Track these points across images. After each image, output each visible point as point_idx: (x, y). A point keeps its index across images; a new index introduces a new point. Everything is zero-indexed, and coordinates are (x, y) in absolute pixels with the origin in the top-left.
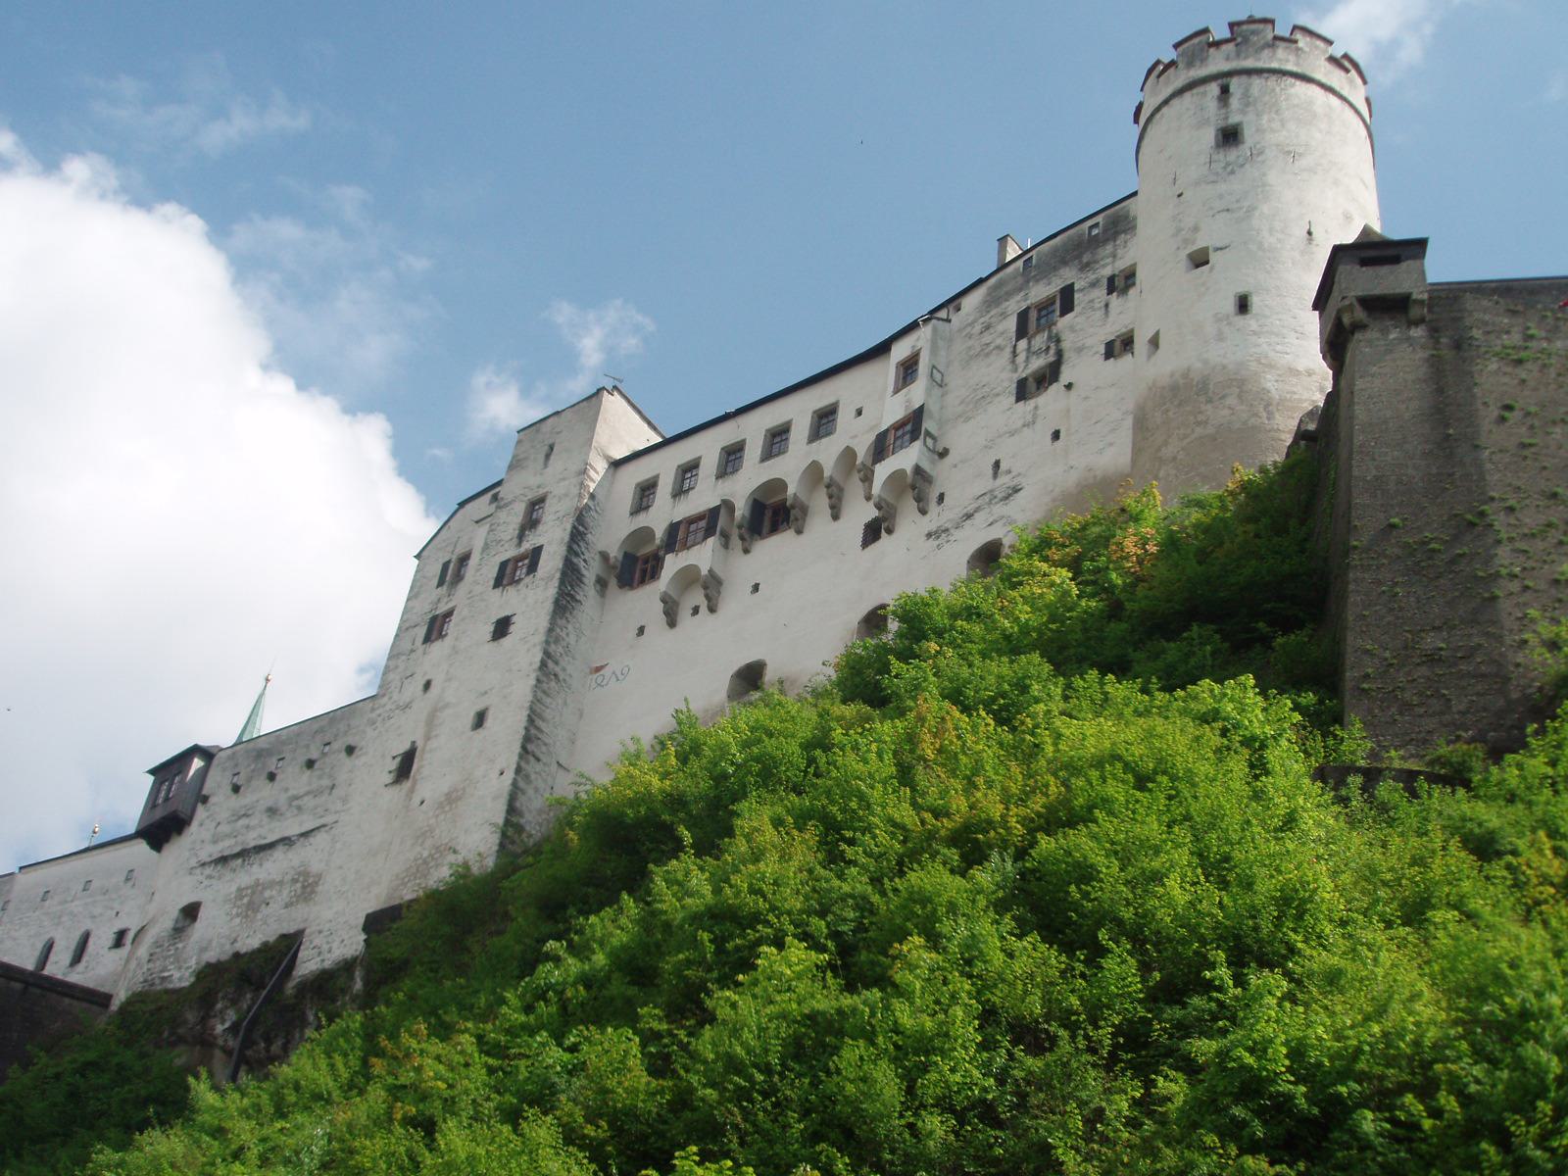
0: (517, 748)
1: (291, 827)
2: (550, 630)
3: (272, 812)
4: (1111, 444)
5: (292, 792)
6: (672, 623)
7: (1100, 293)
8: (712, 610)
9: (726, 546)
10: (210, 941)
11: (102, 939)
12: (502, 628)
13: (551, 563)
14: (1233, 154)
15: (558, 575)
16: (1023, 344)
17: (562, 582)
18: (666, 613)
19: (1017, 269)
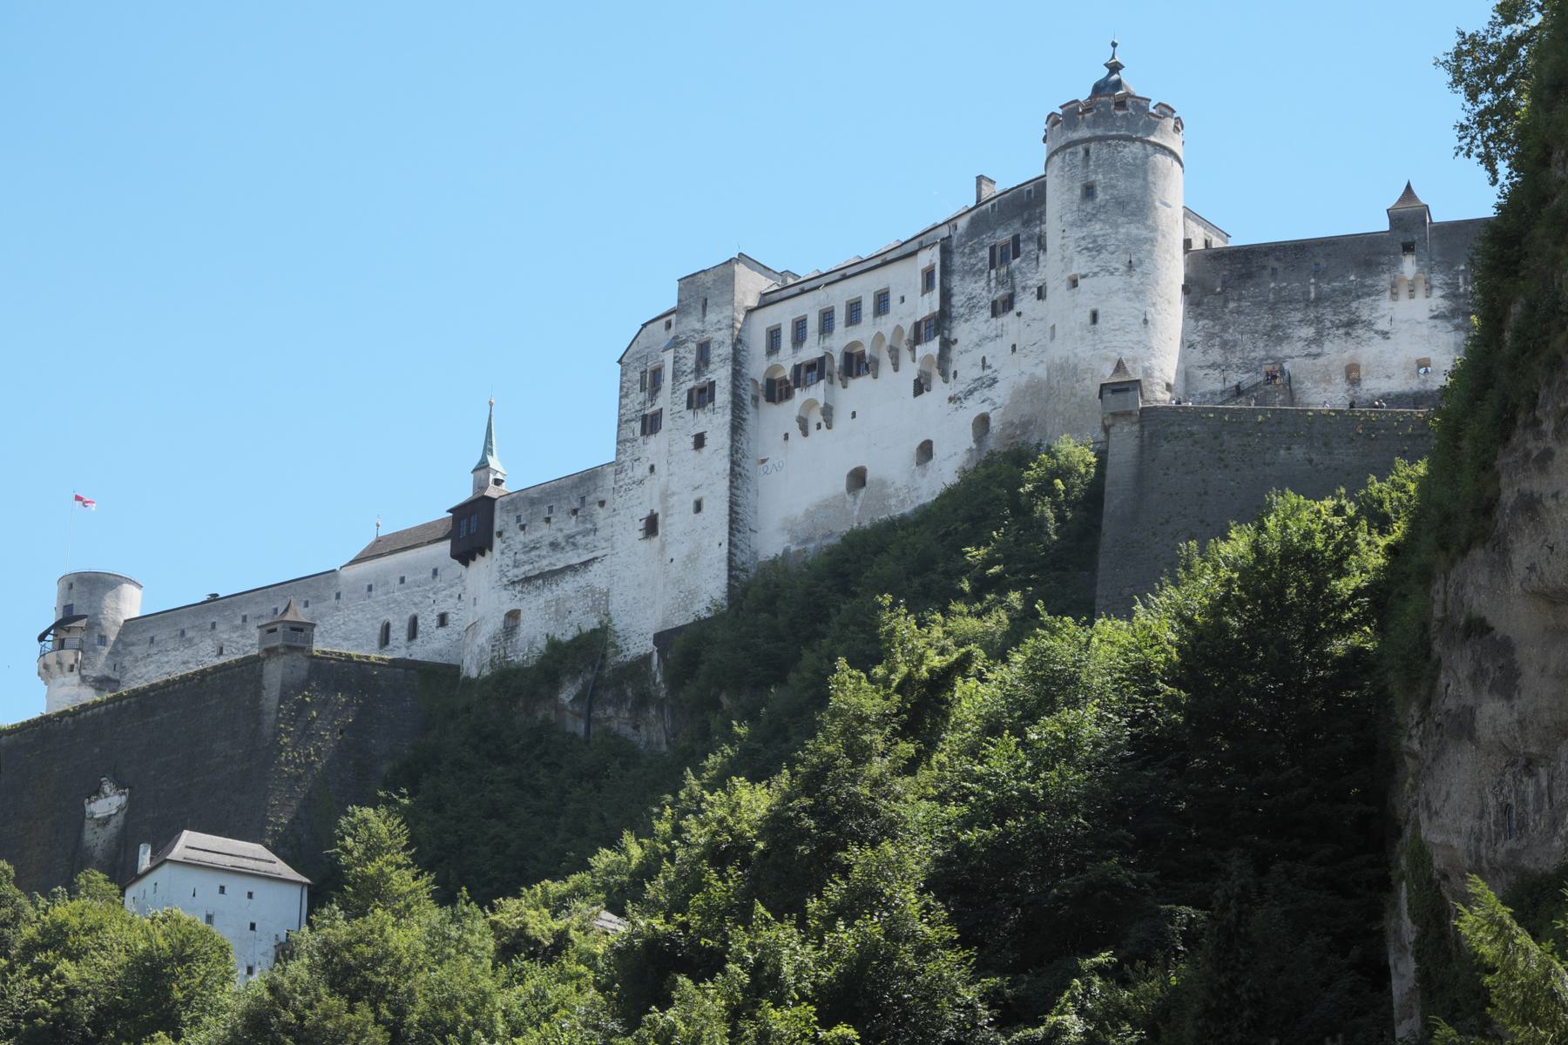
0: (726, 528)
1: (575, 561)
2: (732, 446)
3: (554, 546)
4: (1042, 362)
5: (566, 532)
6: (805, 434)
7: (1033, 246)
8: (829, 427)
9: (831, 382)
10: (535, 637)
11: (428, 621)
12: (699, 441)
13: (723, 396)
14: (1089, 207)
15: (730, 406)
16: (993, 272)
17: (733, 411)
18: (801, 429)
19: (987, 209)
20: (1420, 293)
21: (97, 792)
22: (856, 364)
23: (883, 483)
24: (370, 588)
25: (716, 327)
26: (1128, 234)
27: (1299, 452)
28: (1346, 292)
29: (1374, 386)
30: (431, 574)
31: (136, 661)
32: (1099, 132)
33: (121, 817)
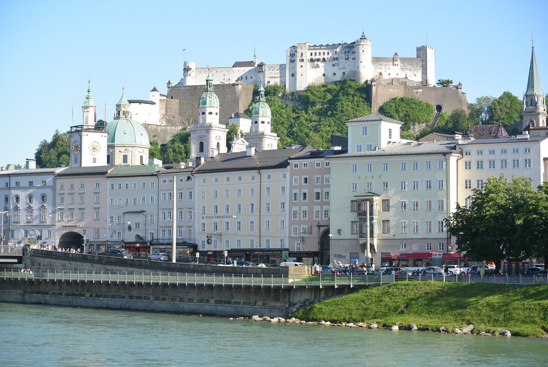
11: (249, 77)
12: (302, 66)
14: (363, 53)
25: (303, 51)
29: (392, 76)
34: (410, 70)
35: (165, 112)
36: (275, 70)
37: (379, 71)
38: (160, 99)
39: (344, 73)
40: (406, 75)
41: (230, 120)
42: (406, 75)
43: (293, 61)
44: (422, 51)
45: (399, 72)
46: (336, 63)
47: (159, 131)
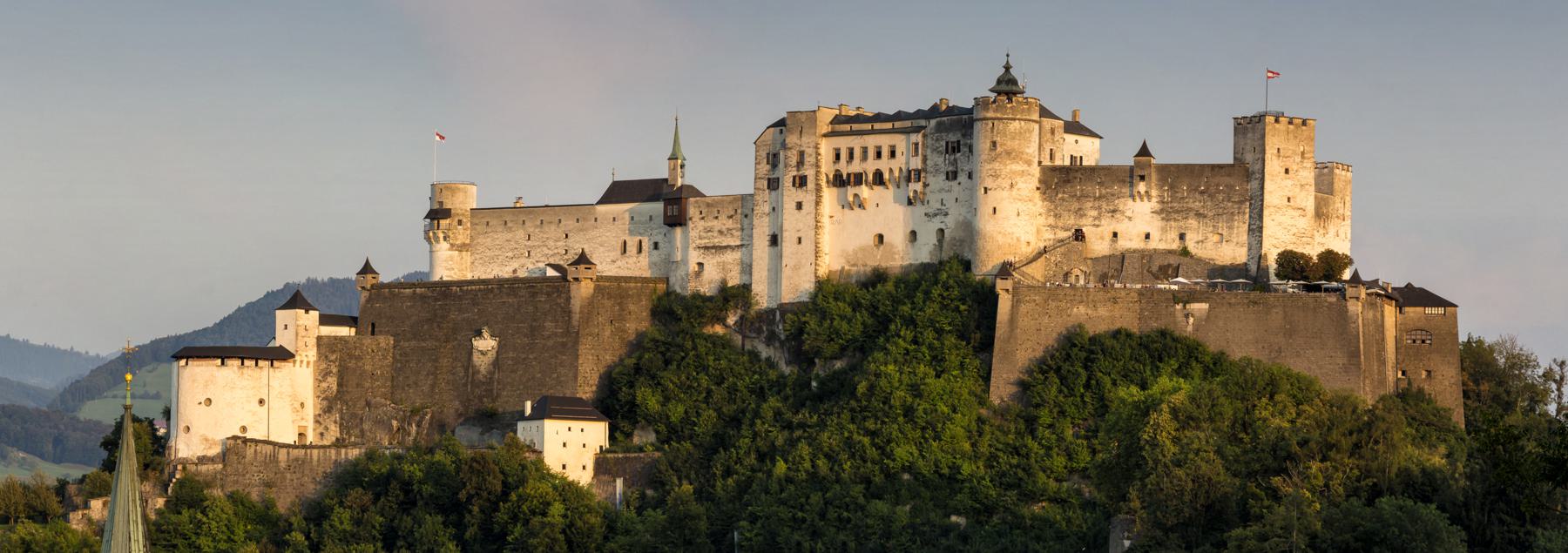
1: (732, 244)
3: (721, 232)
5: (727, 226)
7: (967, 149)
12: (799, 206)
20: (1145, 199)
21: (479, 334)
22: (879, 179)
23: (892, 246)
24: (614, 219)
26: (1011, 170)
27: (1082, 309)
28: (1113, 195)
29: (1124, 244)
30: (648, 218)
31: (479, 234)
32: (999, 115)
33: (494, 352)
34: (1199, 215)
35: (335, 388)
36: (723, 217)
37: (1072, 221)
38: (319, 338)
39: (942, 231)
40: (1182, 237)
41: (521, 425)
42: (1182, 237)
43: (773, 184)
44: (1250, 135)
45: (1154, 226)
46: (915, 192)
47: (283, 465)
